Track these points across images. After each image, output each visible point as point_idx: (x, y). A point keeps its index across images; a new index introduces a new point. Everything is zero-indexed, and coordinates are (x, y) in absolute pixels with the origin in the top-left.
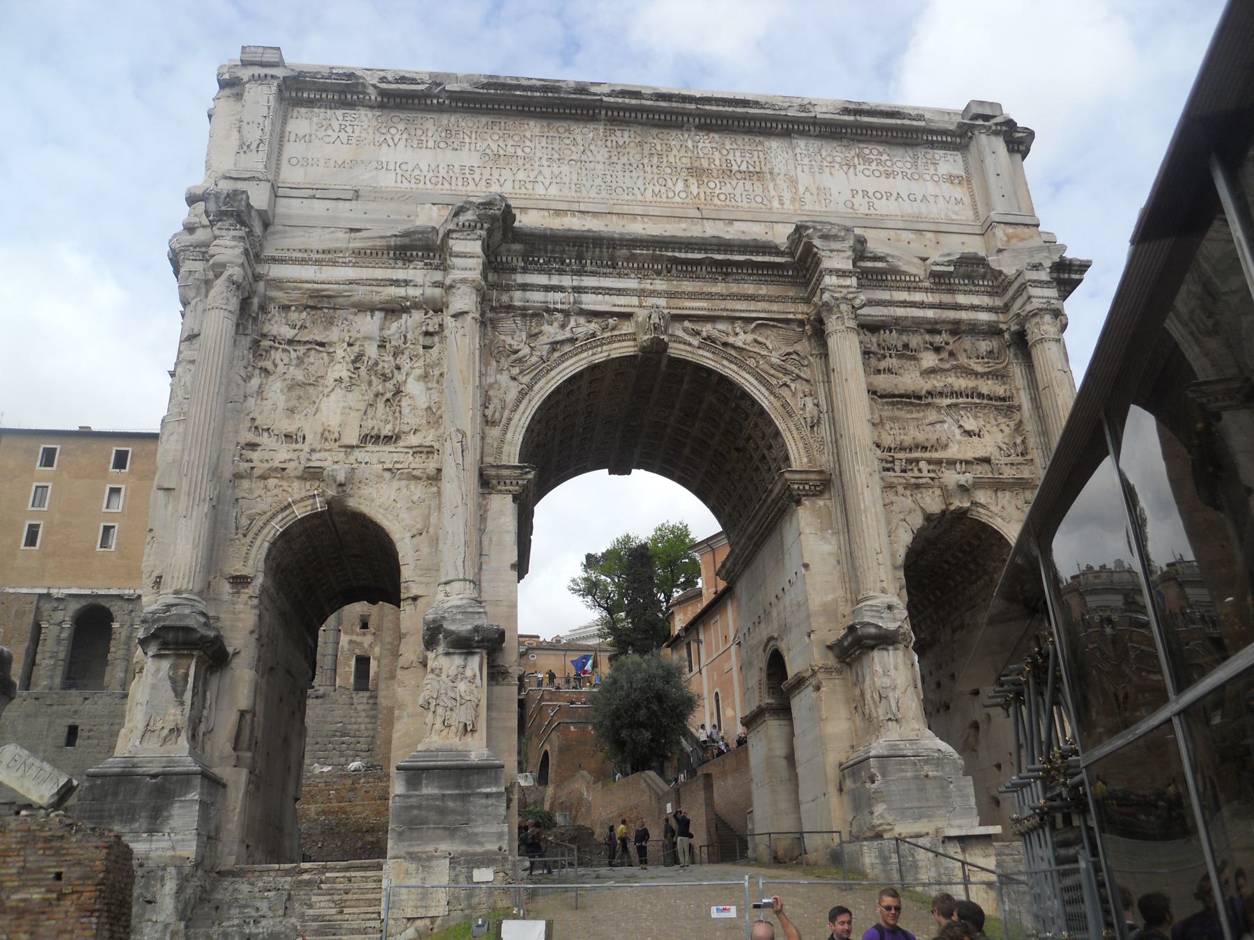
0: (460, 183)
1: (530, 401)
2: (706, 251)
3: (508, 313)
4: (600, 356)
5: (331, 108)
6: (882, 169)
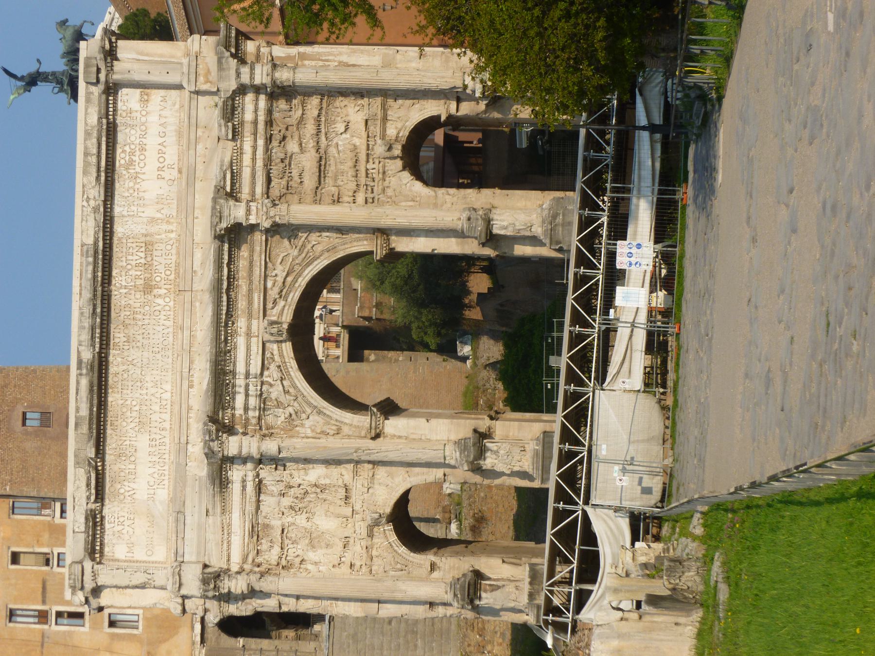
0: (164, 448)
1: (324, 408)
2: (221, 293)
4: (293, 364)
6: (138, 153)
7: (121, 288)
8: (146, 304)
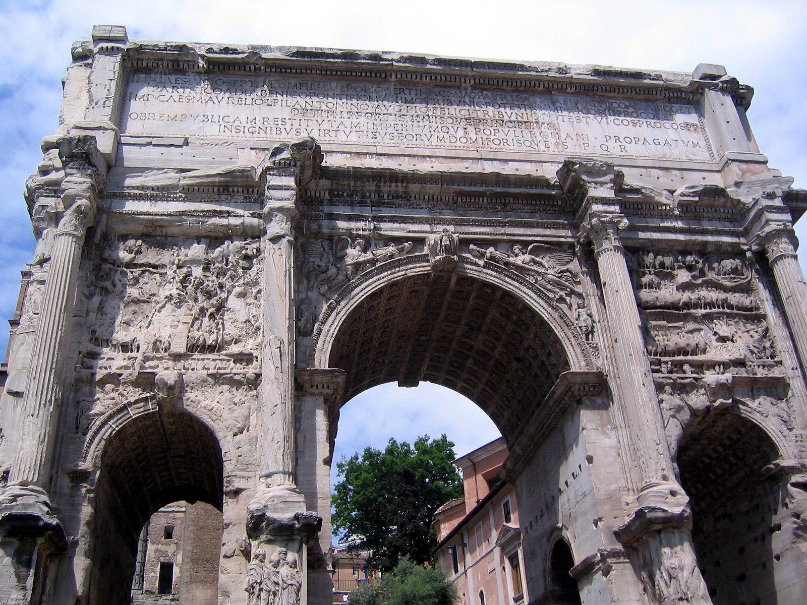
0: (274, 131)
3: (316, 239)
4: (399, 274)
5: (165, 74)
7: (470, 98)
8: (455, 120)
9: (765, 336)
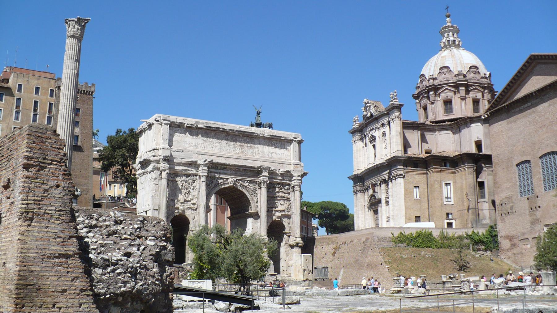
9: (290, 205)
